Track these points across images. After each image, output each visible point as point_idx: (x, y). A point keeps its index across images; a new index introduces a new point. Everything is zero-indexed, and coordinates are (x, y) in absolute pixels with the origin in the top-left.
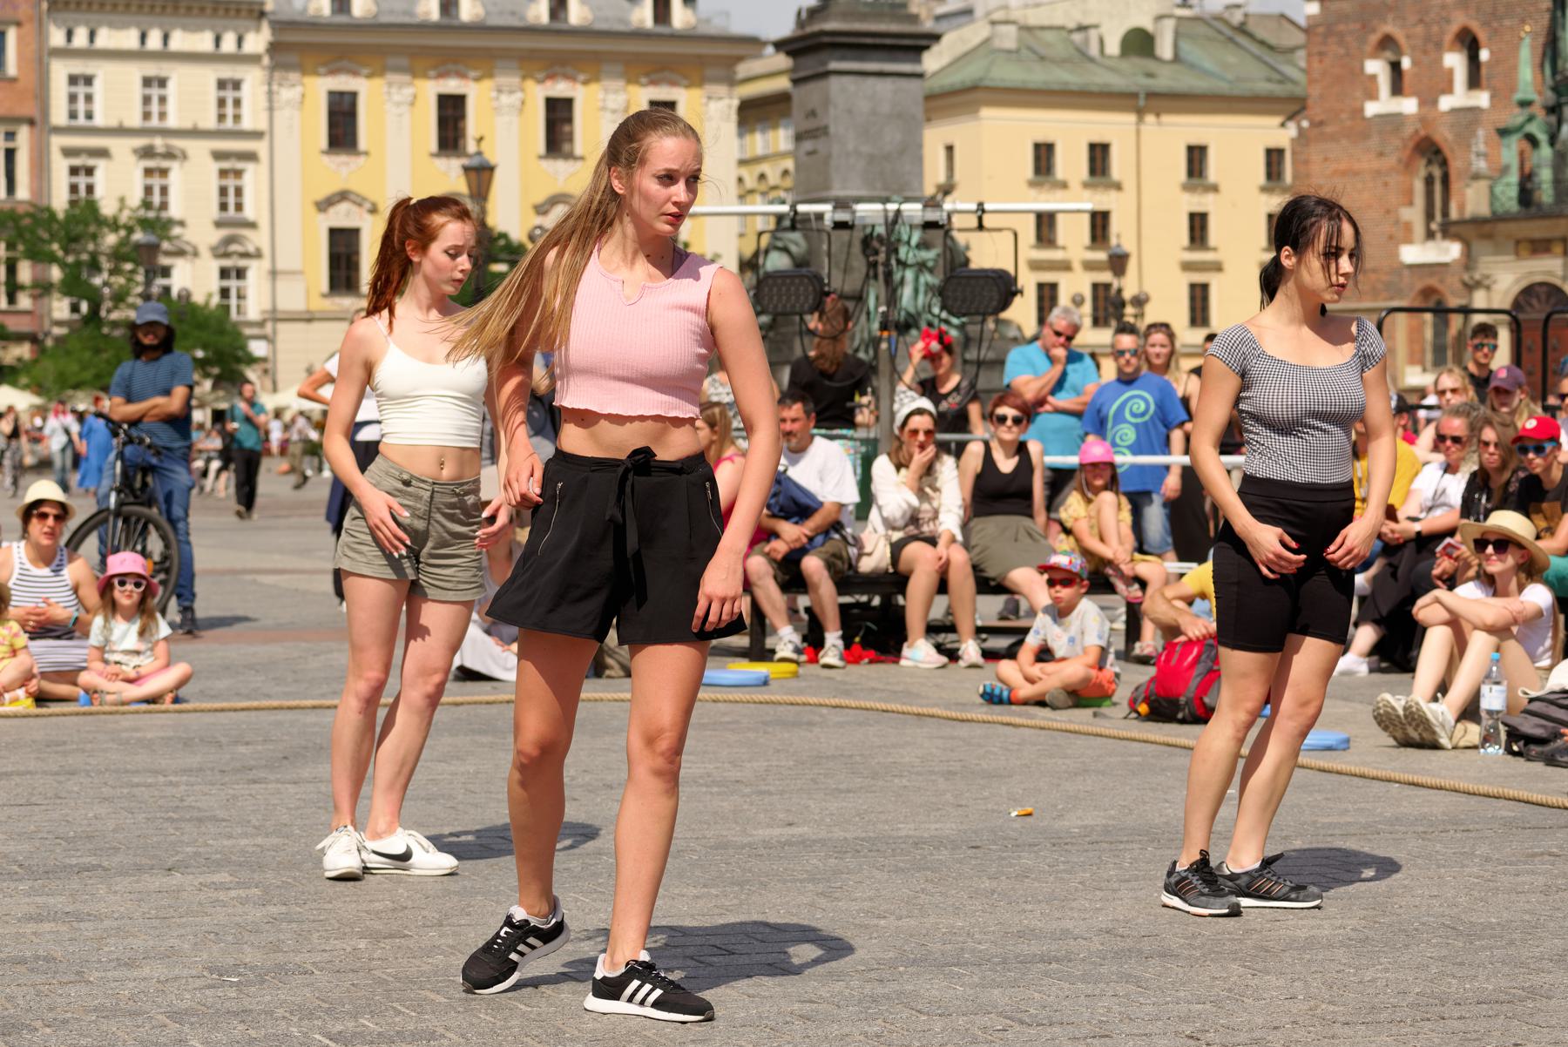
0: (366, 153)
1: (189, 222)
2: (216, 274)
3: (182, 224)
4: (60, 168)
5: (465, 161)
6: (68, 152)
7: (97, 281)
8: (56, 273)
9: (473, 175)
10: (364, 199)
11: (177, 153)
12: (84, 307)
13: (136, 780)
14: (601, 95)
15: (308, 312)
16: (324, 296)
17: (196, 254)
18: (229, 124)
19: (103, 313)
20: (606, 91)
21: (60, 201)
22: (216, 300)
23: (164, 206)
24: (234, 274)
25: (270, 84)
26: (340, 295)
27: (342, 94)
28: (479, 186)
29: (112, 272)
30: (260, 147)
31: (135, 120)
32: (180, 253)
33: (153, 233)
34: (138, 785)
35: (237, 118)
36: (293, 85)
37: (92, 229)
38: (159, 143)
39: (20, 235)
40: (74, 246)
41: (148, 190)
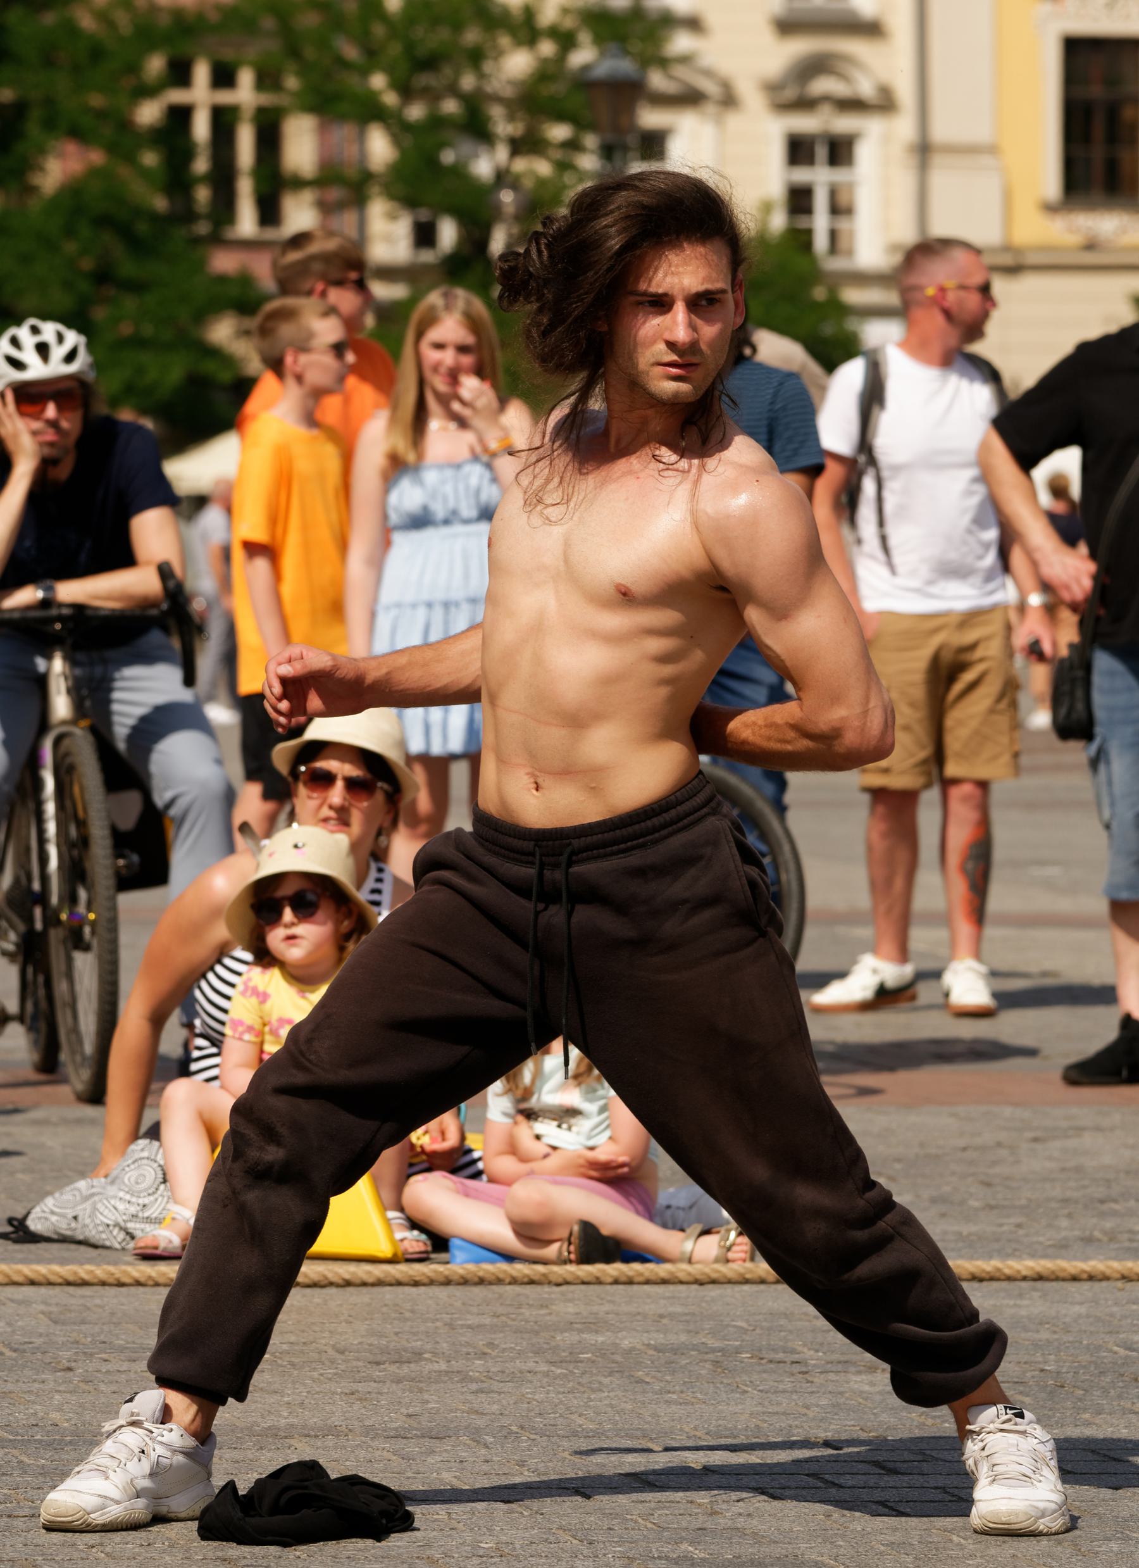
1: (712, 18)
2: (777, 152)
3: (694, 24)
7: (483, 167)
8: (380, 148)
12: (448, 233)
15: (1007, 248)
16: (1050, 209)
17: (729, 100)
22: (778, 221)
24: (821, 152)
26: (1091, 206)
29: (518, 147)
32: (690, 98)
33: (626, 53)
37: (472, 36)
39: (293, 51)
40: (424, 79)
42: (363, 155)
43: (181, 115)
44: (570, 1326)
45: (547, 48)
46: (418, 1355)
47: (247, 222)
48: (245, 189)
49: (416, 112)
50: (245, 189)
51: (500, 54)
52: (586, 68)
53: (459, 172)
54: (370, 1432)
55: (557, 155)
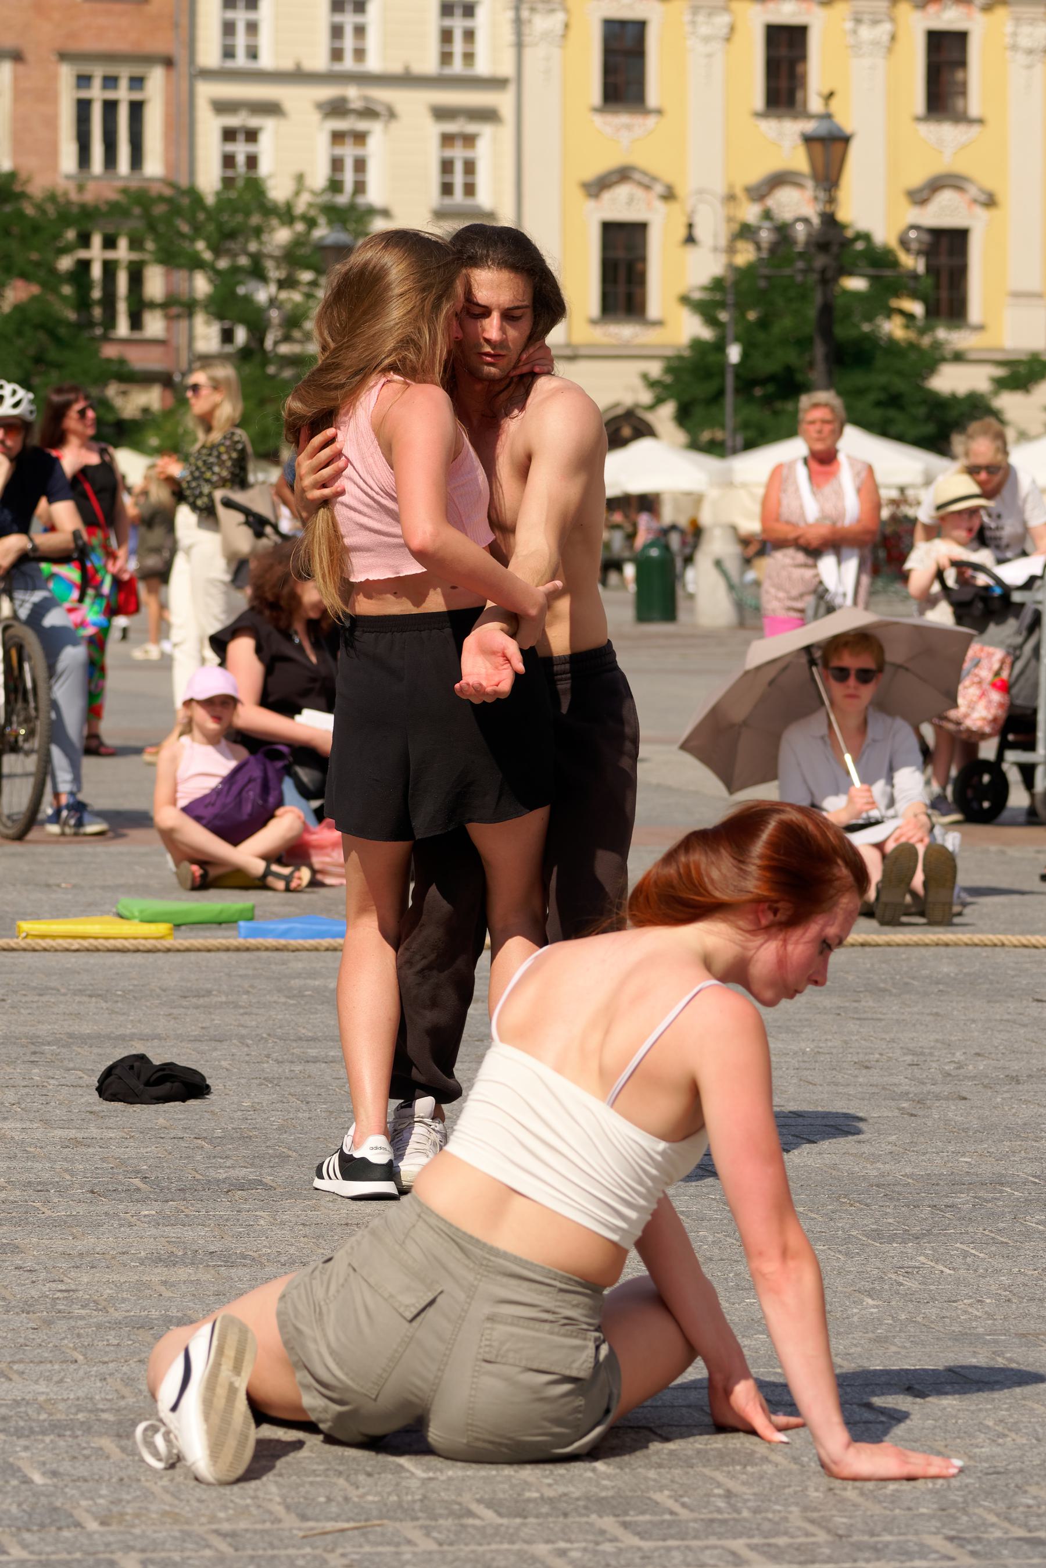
0: (659, 112)
4: (209, 128)
5: (809, 126)
6: (221, 107)
7: (262, 295)
8: (202, 285)
9: (818, 148)
10: (655, 179)
11: (379, 108)
12: (241, 335)
13: (313, 1052)
14: (1009, 27)
15: (568, 345)
16: (593, 322)
18: (457, 67)
19: (269, 343)
20: (1018, 20)
21: (209, 179)
23: (360, 187)
25: (517, 9)
26: (618, 321)
27: (623, 23)
28: (827, 165)
29: (282, 284)
30: (503, 101)
31: (319, 60)
33: (346, 229)
34: (315, 1060)
35: (469, 57)
36: (552, 11)
37: (255, 220)
38: (353, 93)
41: (337, 164)
42: (192, 289)
43: (84, 265)
44: (299, 976)
45: (300, 227)
46: (209, 993)
47: (123, 328)
48: (122, 308)
49: (223, 264)
50: (122, 308)
51: (272, 230)
52: (322, 238)
53: (248, 299)
54: (180, 1038)
55: (305, 289)
